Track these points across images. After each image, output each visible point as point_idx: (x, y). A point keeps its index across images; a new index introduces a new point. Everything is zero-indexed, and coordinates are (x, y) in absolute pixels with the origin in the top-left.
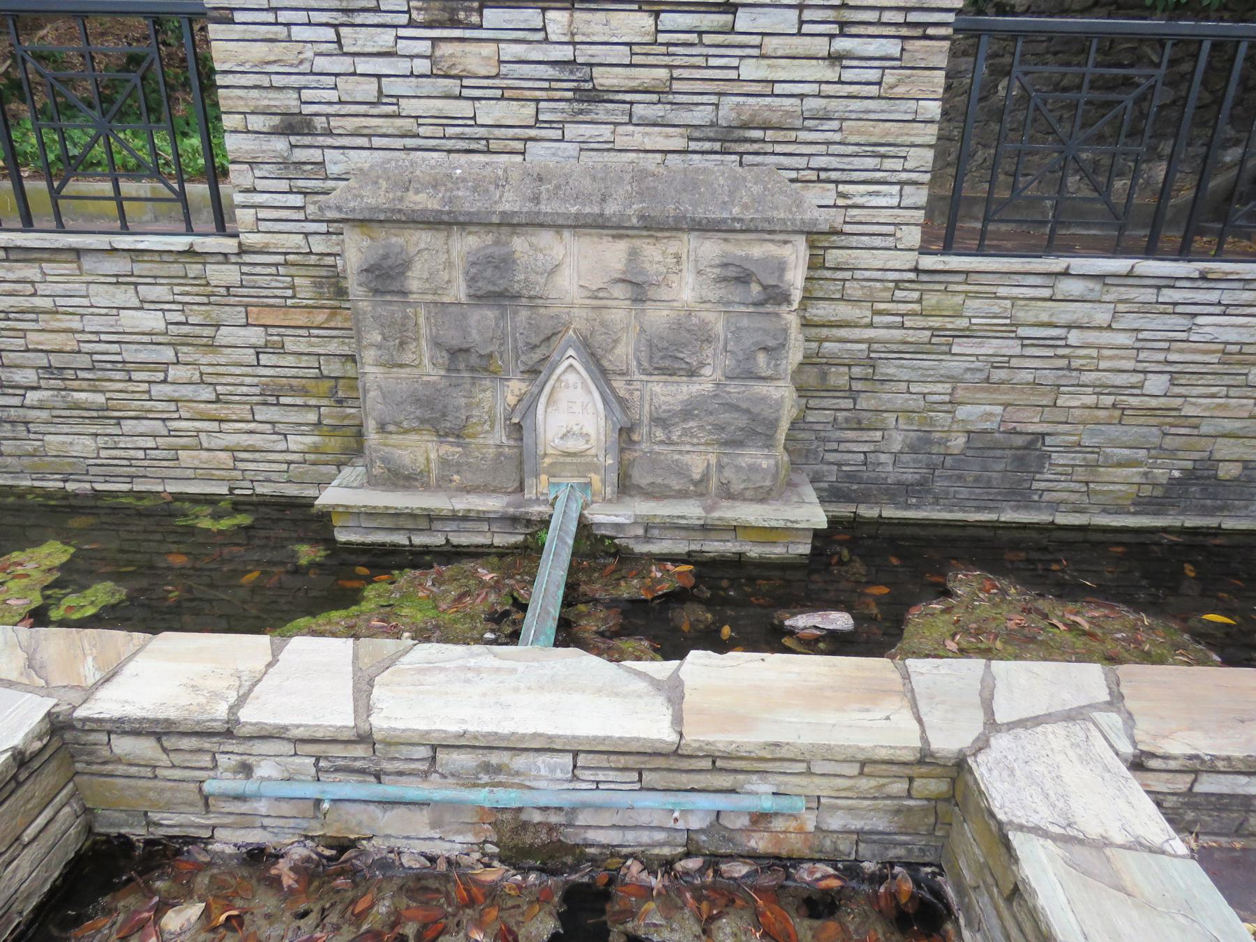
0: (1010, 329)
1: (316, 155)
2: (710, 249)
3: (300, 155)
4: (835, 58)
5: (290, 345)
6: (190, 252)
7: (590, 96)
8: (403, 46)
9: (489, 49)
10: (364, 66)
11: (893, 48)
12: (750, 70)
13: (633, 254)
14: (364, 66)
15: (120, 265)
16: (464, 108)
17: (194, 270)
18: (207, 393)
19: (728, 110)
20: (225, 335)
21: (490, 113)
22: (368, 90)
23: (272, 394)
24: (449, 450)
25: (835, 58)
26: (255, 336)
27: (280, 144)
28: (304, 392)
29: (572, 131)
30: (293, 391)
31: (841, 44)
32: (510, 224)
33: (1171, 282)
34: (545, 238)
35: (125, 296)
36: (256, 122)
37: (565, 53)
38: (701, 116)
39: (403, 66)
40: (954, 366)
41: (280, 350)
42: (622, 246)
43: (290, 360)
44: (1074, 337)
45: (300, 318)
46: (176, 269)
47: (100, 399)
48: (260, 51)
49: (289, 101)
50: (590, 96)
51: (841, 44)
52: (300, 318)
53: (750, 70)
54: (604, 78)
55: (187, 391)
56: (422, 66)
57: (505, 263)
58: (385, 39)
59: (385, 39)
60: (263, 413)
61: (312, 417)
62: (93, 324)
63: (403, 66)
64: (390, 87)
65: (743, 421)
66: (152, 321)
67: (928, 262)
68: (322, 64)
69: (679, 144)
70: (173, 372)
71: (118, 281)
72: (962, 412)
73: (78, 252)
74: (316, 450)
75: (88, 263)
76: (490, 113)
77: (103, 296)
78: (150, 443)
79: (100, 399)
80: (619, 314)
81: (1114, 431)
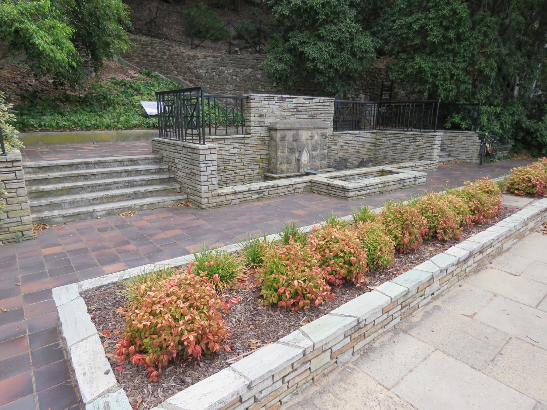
0: (342, 142)
1: (263, 120)
2: (320, 131)
3: (261, 120)
4: (323, 106)
5: (256, 153)
6: (244, 138)
7: (298, 111)
8: (276, 104)
9: (286, 104)
10: (271, 107)
11: (328, 104)
12: (315, 107)
13: (312, 133)
14: (271, 107)
15: (231, 141)
16: (283, 113)
17: (243, 141)
18: (242, 164)
19: (313, 112)
20: (247, 152)
21: (286, 113)
22: (271, 110)
23: (252, 163)
24: (288, 166)
25: (323, 106)
26: (251, 152)
27: (259, 119)
28: (258, 162)
29: (296, 116)
30: (256, 162)
31: (324, 104)
32: (299, 129)
33: (356, 134)
34: (301, 131)
35: (231, 147)
36: (256, 115)
38: (310, 113)
39: (276, 107)
40: (338, 148)
41: (254, 154)
42: (310, 132)
43: (256, 156)
44: (349, 142)
45: (258, 148)
46: (240, 141)
47: (223, 168)
48: (257, 104)
49: (261, 112)
50: (298, 111)
51: (324, 104)
52: (258, 148)
53: (315, 107)
54: (300, 108)
55: (239, 164)
56: (278, 107)
57: (298, 135)
58: (274, 103)
59: (274, 103)
60: (251, 167)
61: (258, 166)
62: (225, 152)
63: (276, 107)
64: (275, 110)
65: (323, 156)
66: (235, 151)
67: (334, 133)
68: (266, 106)
70: (237, 161)
71: (230, 144)
72: (339, 154)
73: (225, 139)
74: (258, 173)
75: (226, 141)
76: (286, 113)
77: (228, 147)
78: (231, 176)
79: (223, 168)
80: (309, 142)
81: (354, 155)
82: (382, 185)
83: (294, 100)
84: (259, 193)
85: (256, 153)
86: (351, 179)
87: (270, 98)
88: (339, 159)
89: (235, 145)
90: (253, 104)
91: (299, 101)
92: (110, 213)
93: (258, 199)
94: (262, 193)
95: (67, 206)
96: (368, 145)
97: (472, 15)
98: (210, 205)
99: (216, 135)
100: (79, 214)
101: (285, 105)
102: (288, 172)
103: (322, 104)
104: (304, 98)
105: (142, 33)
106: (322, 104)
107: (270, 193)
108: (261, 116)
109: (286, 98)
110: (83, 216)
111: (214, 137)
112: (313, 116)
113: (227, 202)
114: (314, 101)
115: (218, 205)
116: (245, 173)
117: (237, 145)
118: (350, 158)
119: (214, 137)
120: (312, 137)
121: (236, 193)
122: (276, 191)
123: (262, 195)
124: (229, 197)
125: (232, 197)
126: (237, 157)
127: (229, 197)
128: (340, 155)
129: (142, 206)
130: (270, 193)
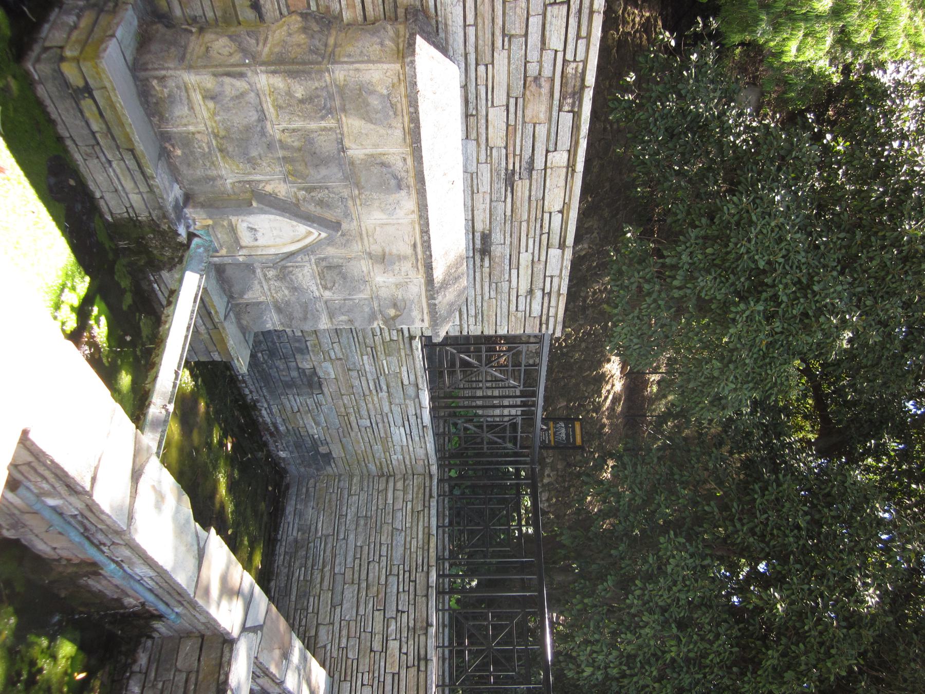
4: (531, 292)
7: (510, 181)
8: (548, 56)
9: (543, 116)
10: (535, 22)
13: (406, 258)
14: (535, 22)
16: (500, 97)
21: (497, 117)
29: (485, 170)
31: (538, 294)
37: (539, 164)
39: (533, 55)
42: (409, 251)
50: (510, 181)
53: (525, 258)
54: (521, 187)
56: (533, 69)
58: (555, 42)
59: (555, 42)
63: (533, 55)
64: (518, 42)
67: (417, 344)
69: (479, 227)
76: (497, 117)
83: (560, 158)
91: (556, 181)
101: (538, 109)
104: (566, 205)
109: (577, 115)
114: (555, 252)
118: (318, 405)
120: (383, 259)
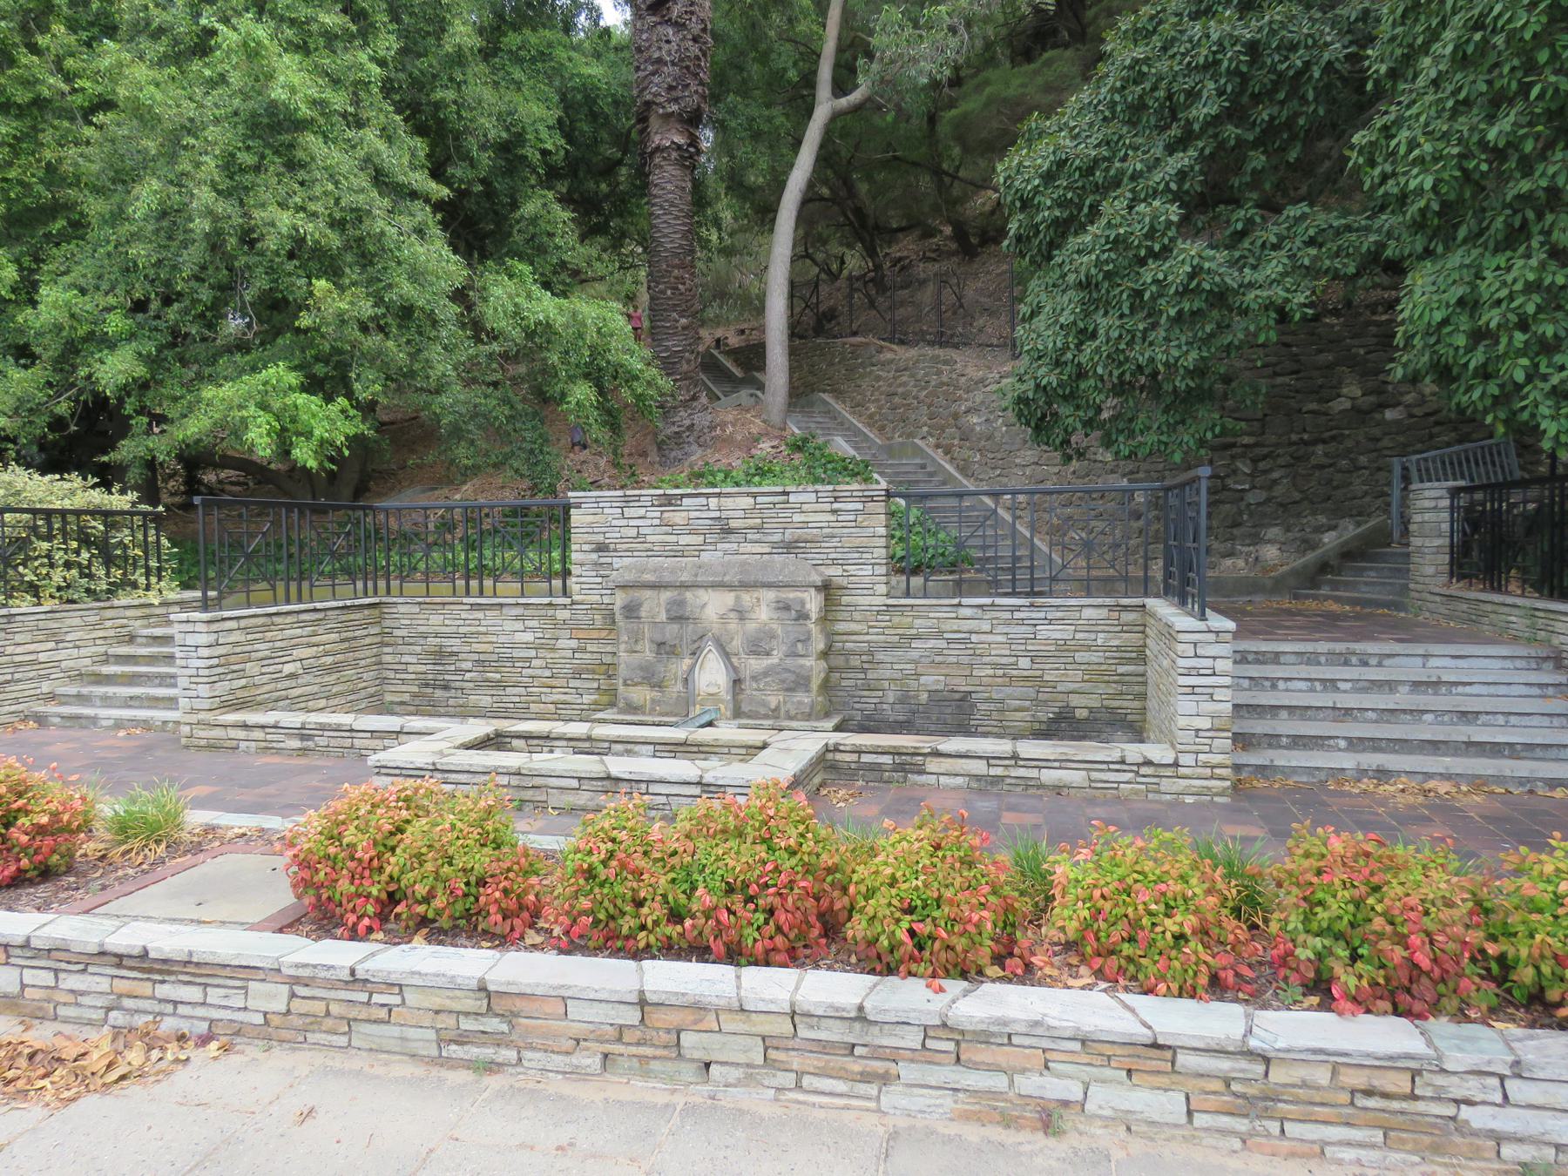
0: (939, 634)
1: (609, 560)
2: (771, 595)
3: (603, 560)
4: (834, 512)
5: (589, 648)
6: (550, 604)
7: (727, 531)
10: (632, 523)
11: (860, 506)
12: (797, 518)
13: (737, 598)
14: (632, 523)
15: (518, 611)
16: (673, 538)
17: (550, 612)
18: (548, 673)
19: (788, 535)
20: (561, 643)
21: (684, 540)
22: (633, 532)
23: (577, 674)
24: (656, 694)
25: (834, 512)
26: (574, 644)
27: (594, 556)
28: (594, 672)
29: (719, 546)
30: (589, 671)
31: (836, 506)
32: (684, 586)
33: (1018, 608)
34: (701, 592)
35: (519, 625)
36: (585, 547)
37: (717, 514)
38: (777, 538)
39: (649, 522)
40: (915, 654)
41: (584, 650)
42: (732, 594)
43: (588, 656)
44: (974, 638)
45: (595, 634)
46: (542, 612)
47: (498, 676)
48: (590, 518)
49: (600, 538)
50: (727, 531)
51: (836, 506)
52: (595, 634)
53: (797, 518)
54: (733, 524)
55: (539, 672)
56: (657, 522)
57: (681, 603)
58: (642, 512)
59: (642, 512)
60: (573, 683)
61: (595, 685)
62: (502, 639)
63: (649, 522)
64: (642, 531)
65: (792, 677)
66: (528, 637)
68: (615, 523)
69: (768, 550)
70: (535, 663)
71: (517, 618)
72: (923, 679)
73: (501, 605)
74: (595, 703)
75: (505, 610)
76: (684, 540)
77: (509, 626)
78: (517, 699)
79: (498, 676)
80: (733, 626)
81: (1009, 690)
82: (515, 781)
83: (713, 502)
84: (303, 738)
85: (589, 648)
86: (617, 754)
87: (627, 501)
88: (924, 697)
89: (530, 624)
90: (576, 517)
91: (728, 503)
92: (119, 724)
93: (303, 751)
94: (309, 737)
95: (98, 703)
96: (1095, 657)
97: (620, 162)
98: (196, 742)
99: (495, 595)
100: (78, 717)
101: (678, 518)
102: (652, 712)
103: (827, 507)
104: (748, 494)
105: (924, 340)
106: (827, 507)
107: (333, 742)
108: (601, 548)
109: (683, 496)
110: (83, 722)
111: (472, 600)
112: (790, 547)
113: (229, 744)
114: (792, 498)
115: (212, 747)
116: (556, 698)
117: (534, 623)
118: (988, 700)
119: (472, 600)
120: (741, 614)
121: (245, 726)
122: (348, 742)
123: (310, 744)
124: (233, 733)
125: (241, 734)
126: (533, 653)
127: (233, 733)
128: (932, 680)
129: (165, 722)
130: (333, 742)
